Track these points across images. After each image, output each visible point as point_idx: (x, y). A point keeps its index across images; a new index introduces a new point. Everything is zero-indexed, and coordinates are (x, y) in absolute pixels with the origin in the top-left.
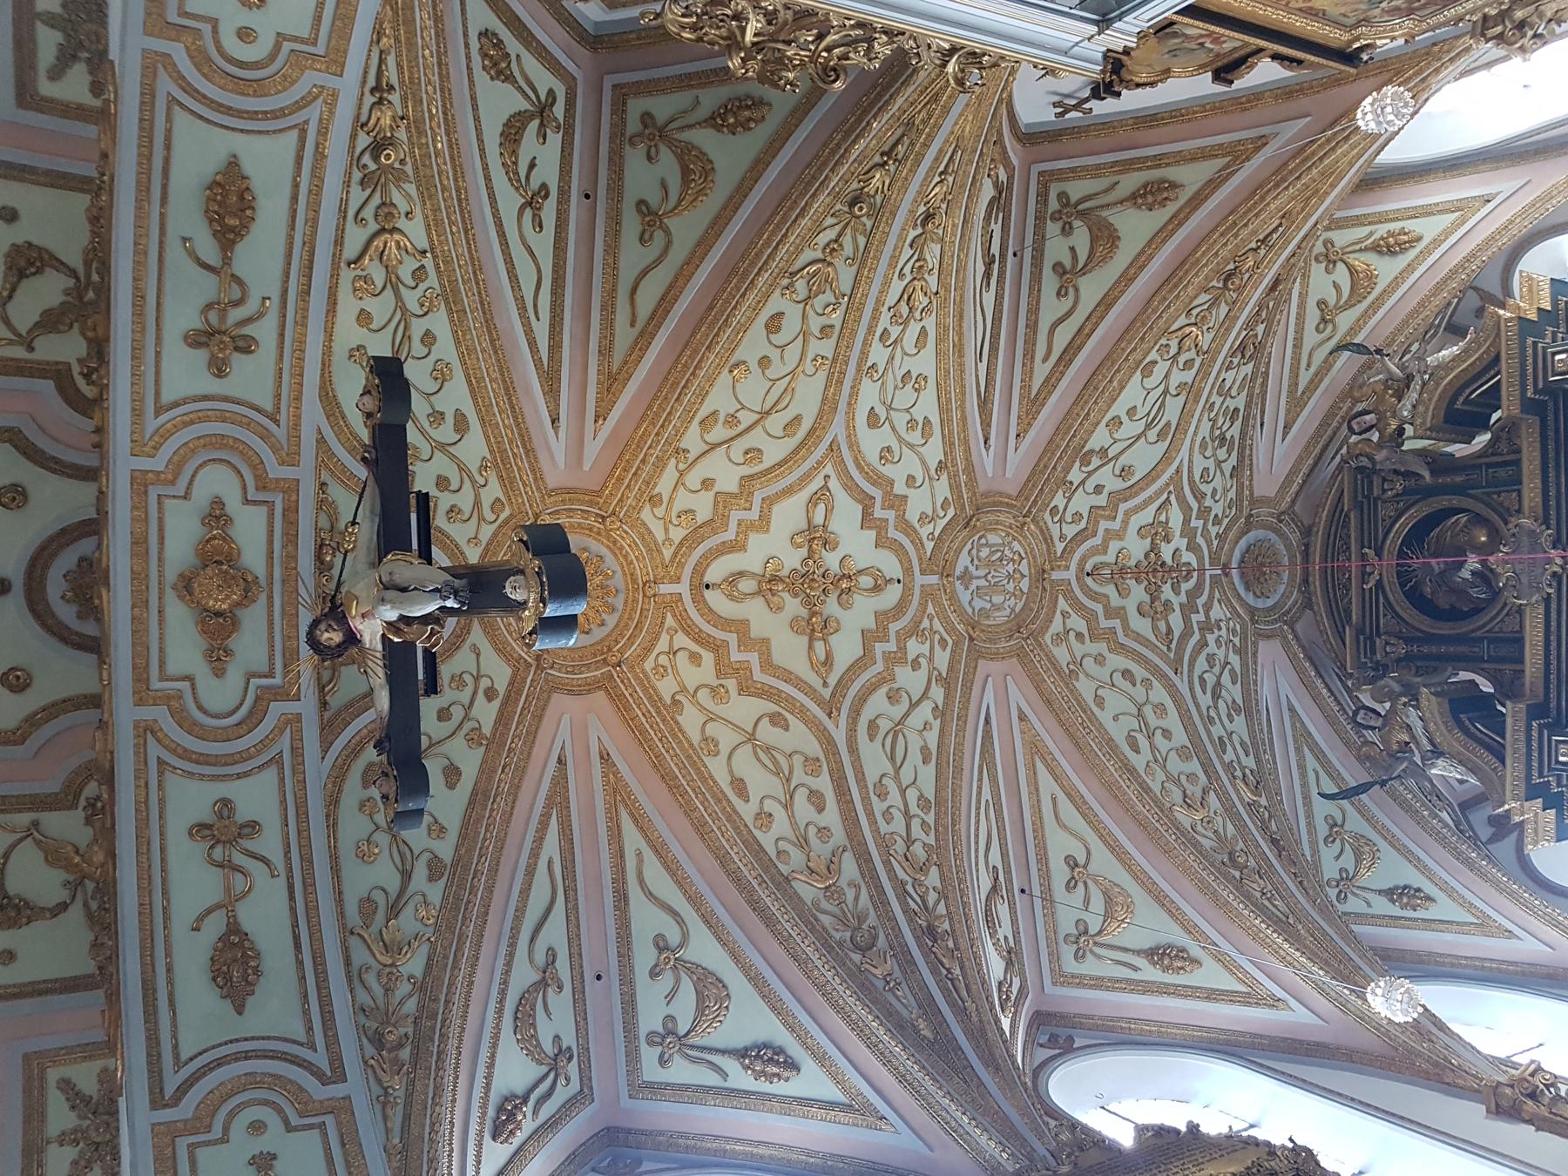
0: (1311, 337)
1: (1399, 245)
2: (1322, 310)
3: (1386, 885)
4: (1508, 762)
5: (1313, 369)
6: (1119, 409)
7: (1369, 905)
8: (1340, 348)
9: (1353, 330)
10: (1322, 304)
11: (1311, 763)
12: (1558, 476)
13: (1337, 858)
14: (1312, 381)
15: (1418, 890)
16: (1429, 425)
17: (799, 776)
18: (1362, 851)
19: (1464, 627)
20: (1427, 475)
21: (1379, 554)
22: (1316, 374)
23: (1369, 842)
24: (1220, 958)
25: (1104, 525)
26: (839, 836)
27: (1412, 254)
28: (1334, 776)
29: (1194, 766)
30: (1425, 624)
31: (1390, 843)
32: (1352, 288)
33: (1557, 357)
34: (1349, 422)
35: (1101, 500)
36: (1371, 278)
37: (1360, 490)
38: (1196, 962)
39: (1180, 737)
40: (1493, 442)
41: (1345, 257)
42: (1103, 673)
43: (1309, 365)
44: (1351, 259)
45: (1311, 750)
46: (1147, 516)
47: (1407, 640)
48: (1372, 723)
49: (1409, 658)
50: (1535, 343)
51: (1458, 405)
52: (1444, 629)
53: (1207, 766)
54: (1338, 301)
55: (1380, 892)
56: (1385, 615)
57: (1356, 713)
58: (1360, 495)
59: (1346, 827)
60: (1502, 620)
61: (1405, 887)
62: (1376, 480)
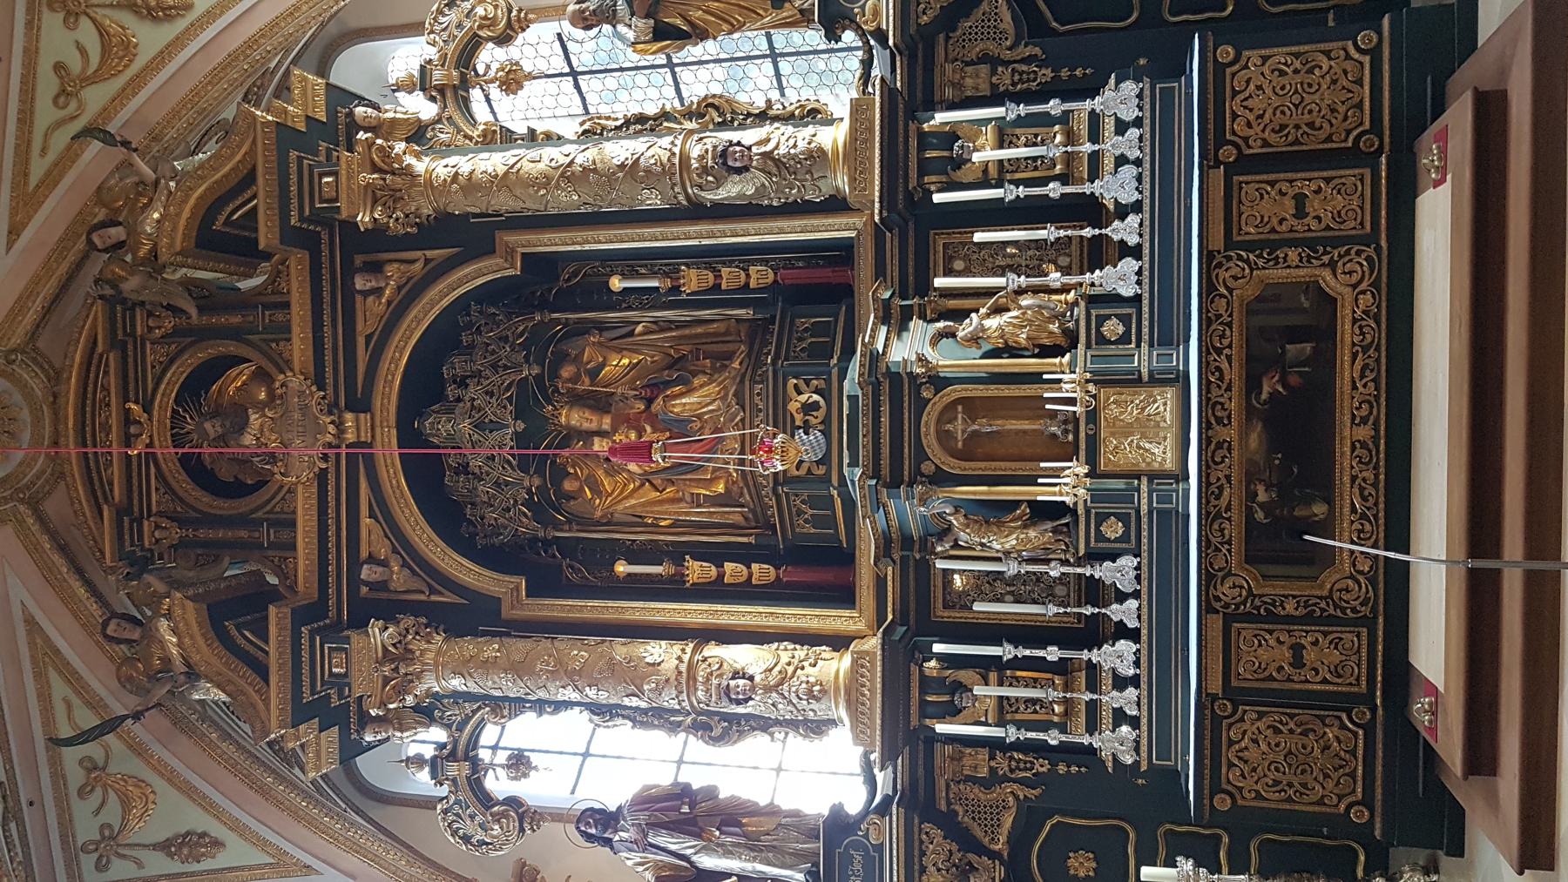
0: (45, 113)
1: (163, 9)
2: (61, 78)
3: (161, 838)
4: (273, 679)
5: (51, 157)
7: (140, 865)
8: (89, 132)
9: (107, 112)
10: (59, 67)
11: (59, 688)
12: (334, 327)
13: (97, 812)
14: (48, 173)
15: (203, 835)
16: (178, 248)
18: (132, 796)
19: (243, 505)
20: (193, 312)
21: (147, 409)
22: (56, 164)
23: (140, 782)
27: (181, 25)
28: (94, 704)
30: (204, 500)
31: (169, 781)
32: (103, 57)
33: (326, 180)
34: (89, 233)
36: (128, 49)
37: (119, 325)
41: (88, 10)
43: (44, 151)
44: (99, 13)
45: (60, 672)
47: (181, 522)
48: (127, 635)
49: (183, 544)
50: (300, 159)
51: (218, 225)
52: (223, 507)
54: (84, 69)
55: (155, 847)
56: (157, 489)
57: (105, 624)
58: (120, 332)
59: (111, 769)
60: (283, 499)
61: (188, 833)
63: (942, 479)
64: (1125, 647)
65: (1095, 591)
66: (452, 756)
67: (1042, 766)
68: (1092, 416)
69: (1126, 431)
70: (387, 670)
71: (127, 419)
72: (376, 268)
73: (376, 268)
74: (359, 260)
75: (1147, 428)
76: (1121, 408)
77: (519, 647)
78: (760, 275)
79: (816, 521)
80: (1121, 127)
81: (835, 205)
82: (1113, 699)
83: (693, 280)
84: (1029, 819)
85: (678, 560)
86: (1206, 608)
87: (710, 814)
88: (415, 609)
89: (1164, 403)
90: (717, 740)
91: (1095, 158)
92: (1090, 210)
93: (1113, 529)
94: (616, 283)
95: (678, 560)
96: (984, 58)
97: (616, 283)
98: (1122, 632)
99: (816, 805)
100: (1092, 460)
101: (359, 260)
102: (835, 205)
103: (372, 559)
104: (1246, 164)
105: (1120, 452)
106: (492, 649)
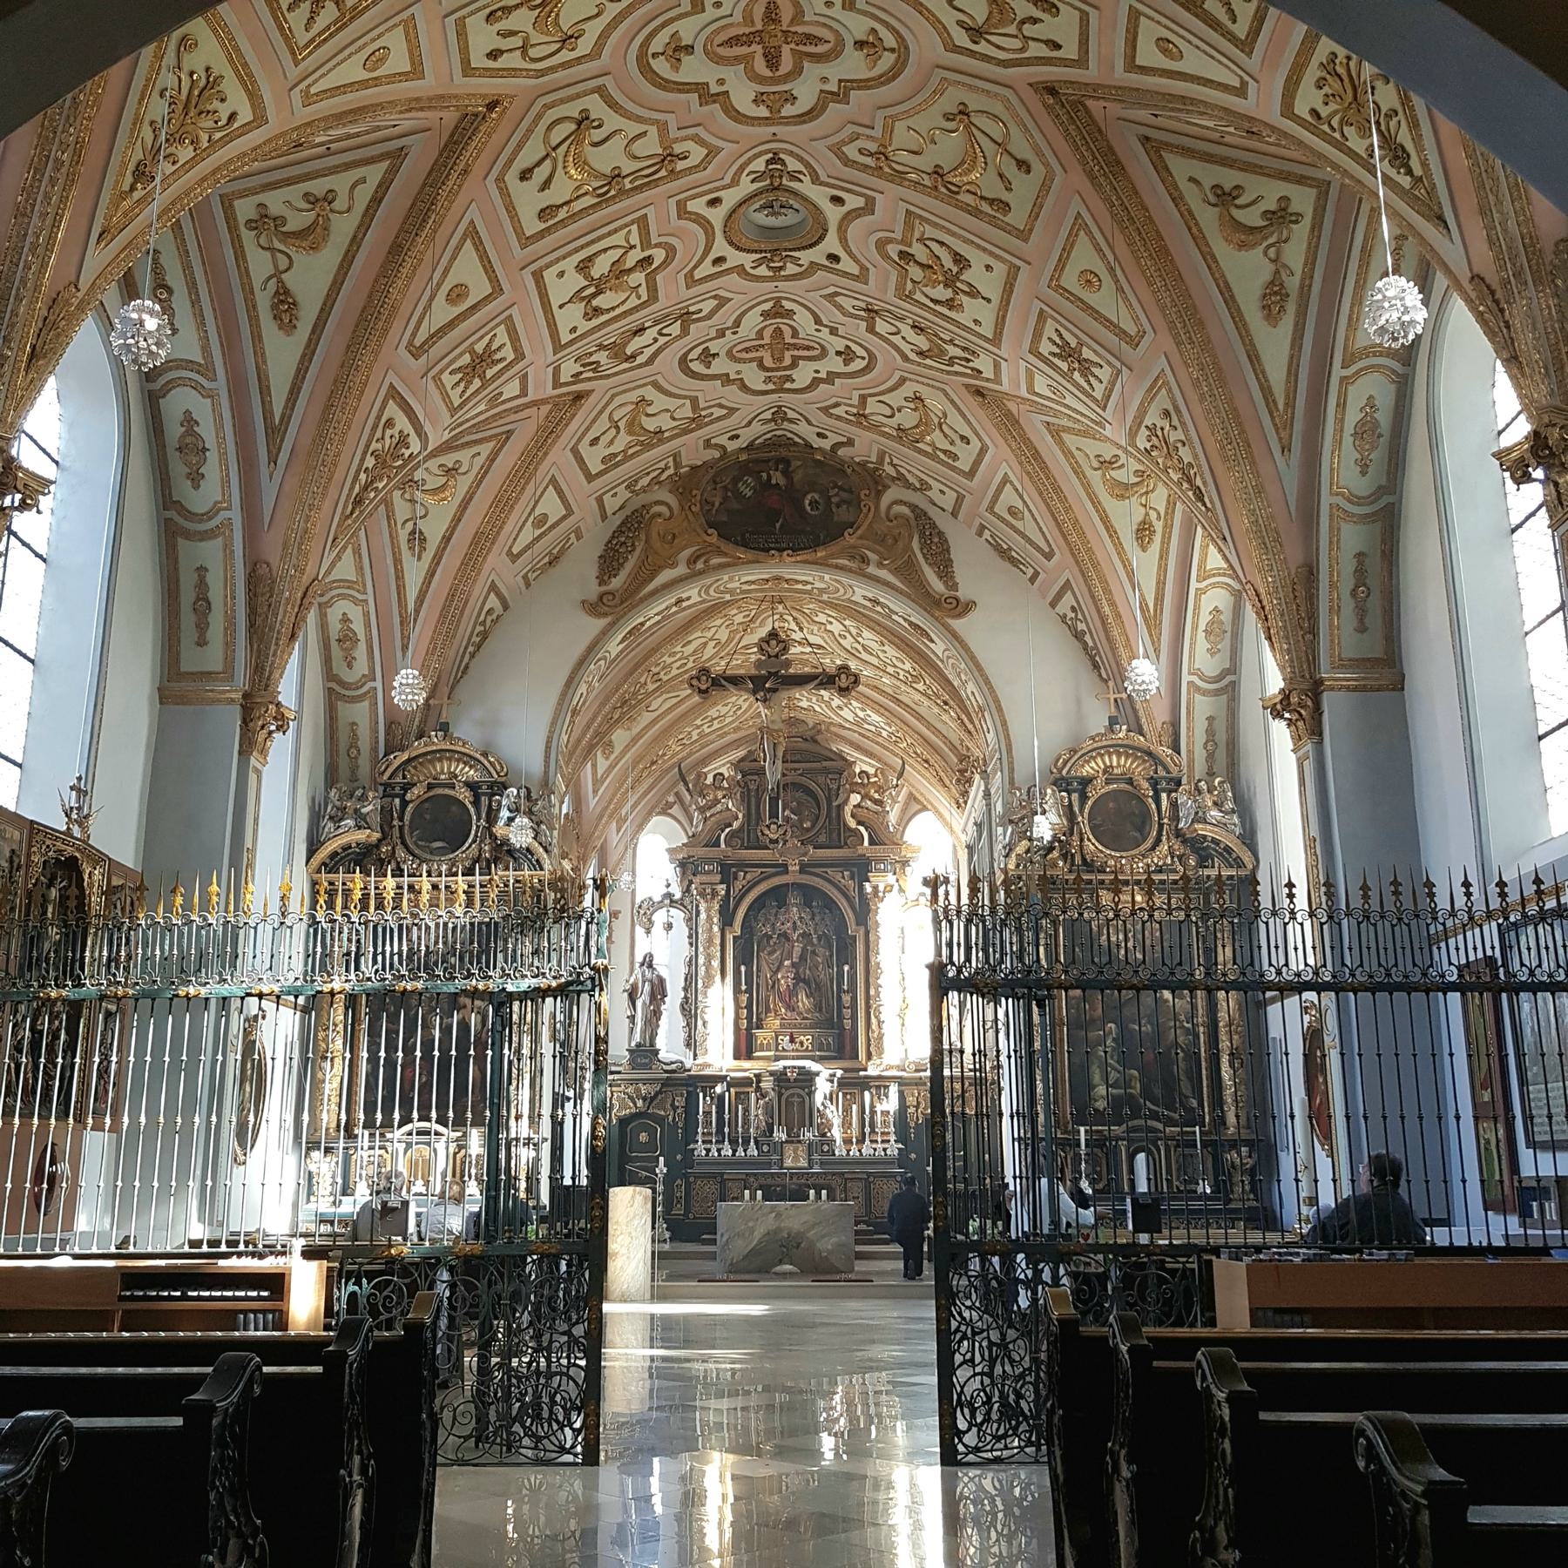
6: (869, 712)
17: (692, 659)
21: (801, 775)
24: (611, 767)
25: (814, 700)
26: (665, 678)
29: (695, 737)
35: (826, 698)
38: (607, 758)
39: (707, 731)
40: (850, 829)
42: (740, 702)
46: (817, 708)
49: (749, 790)
53: (696, 741)
62: (837, 776)
63: (780, 1095)
64: (730, 1153)
65: (746, 1142)
66: (672, 901)
67: (680, 1125)
68: (799, 1142)
69: (795, 1151)
70: (708, 891)
71: (795, 770)
72: (852, 878)
73: (852, 878)
74: (855, 870)
75: (796, 1158)
76: (802, 1151)
77: (718, 941)
78: (847, 1023)
79: (762, 1044)
80: (885, 1150)
81: (869, 1056)
82: (714, 1148)
83: (846, 998)
84: (660, 1120)
85: (746, 992)
86: (747, 1174)
87: (659, 1008)
88: (728, 891)
89: (803, 1163)
90: (682, 1005)
91: (876, 1141)
92: (861, 1141)
93: (765, 1148)
94: (846, 968)
95: (746, 992)
96: (918, 1103)
97: (846, 968)
98: (734, 1151)
99: (661, 1042)
100: (787, 1142)
101: (855, 870)
102: (869, 1056)
103: (746, 873)
104: (868, 1184)
105: (789, 1151)
106: (716, 929)
